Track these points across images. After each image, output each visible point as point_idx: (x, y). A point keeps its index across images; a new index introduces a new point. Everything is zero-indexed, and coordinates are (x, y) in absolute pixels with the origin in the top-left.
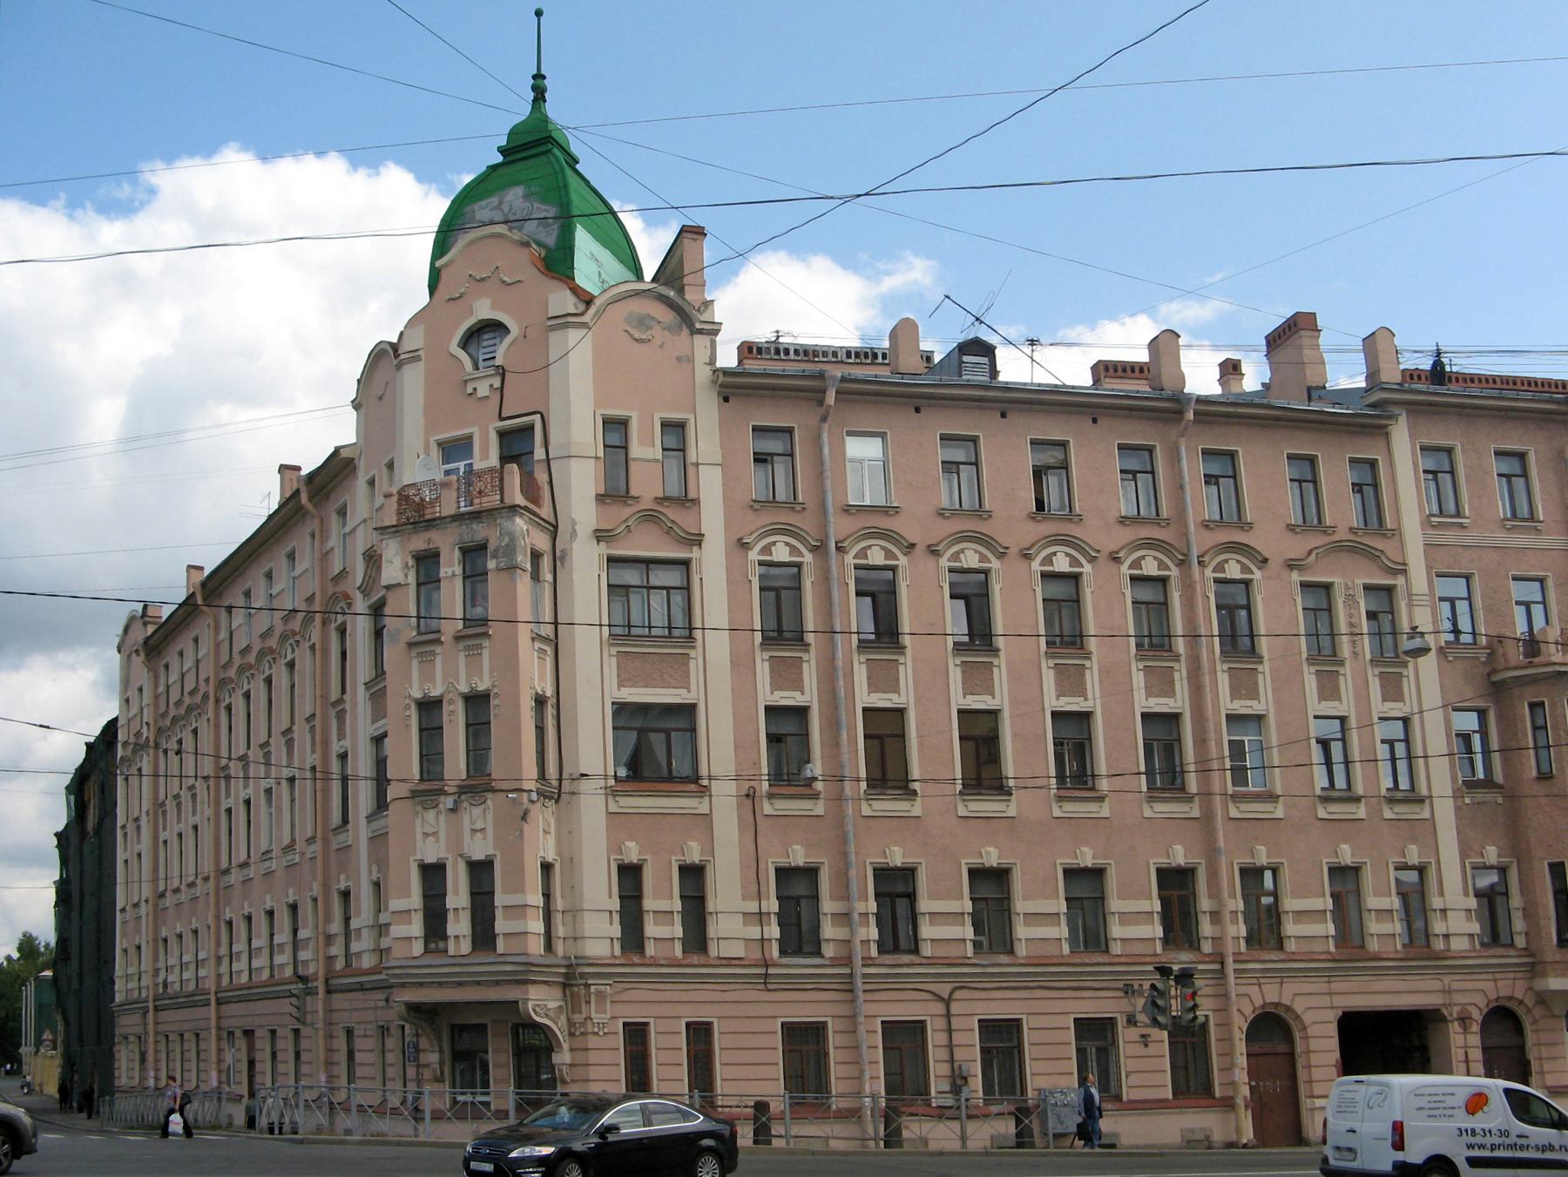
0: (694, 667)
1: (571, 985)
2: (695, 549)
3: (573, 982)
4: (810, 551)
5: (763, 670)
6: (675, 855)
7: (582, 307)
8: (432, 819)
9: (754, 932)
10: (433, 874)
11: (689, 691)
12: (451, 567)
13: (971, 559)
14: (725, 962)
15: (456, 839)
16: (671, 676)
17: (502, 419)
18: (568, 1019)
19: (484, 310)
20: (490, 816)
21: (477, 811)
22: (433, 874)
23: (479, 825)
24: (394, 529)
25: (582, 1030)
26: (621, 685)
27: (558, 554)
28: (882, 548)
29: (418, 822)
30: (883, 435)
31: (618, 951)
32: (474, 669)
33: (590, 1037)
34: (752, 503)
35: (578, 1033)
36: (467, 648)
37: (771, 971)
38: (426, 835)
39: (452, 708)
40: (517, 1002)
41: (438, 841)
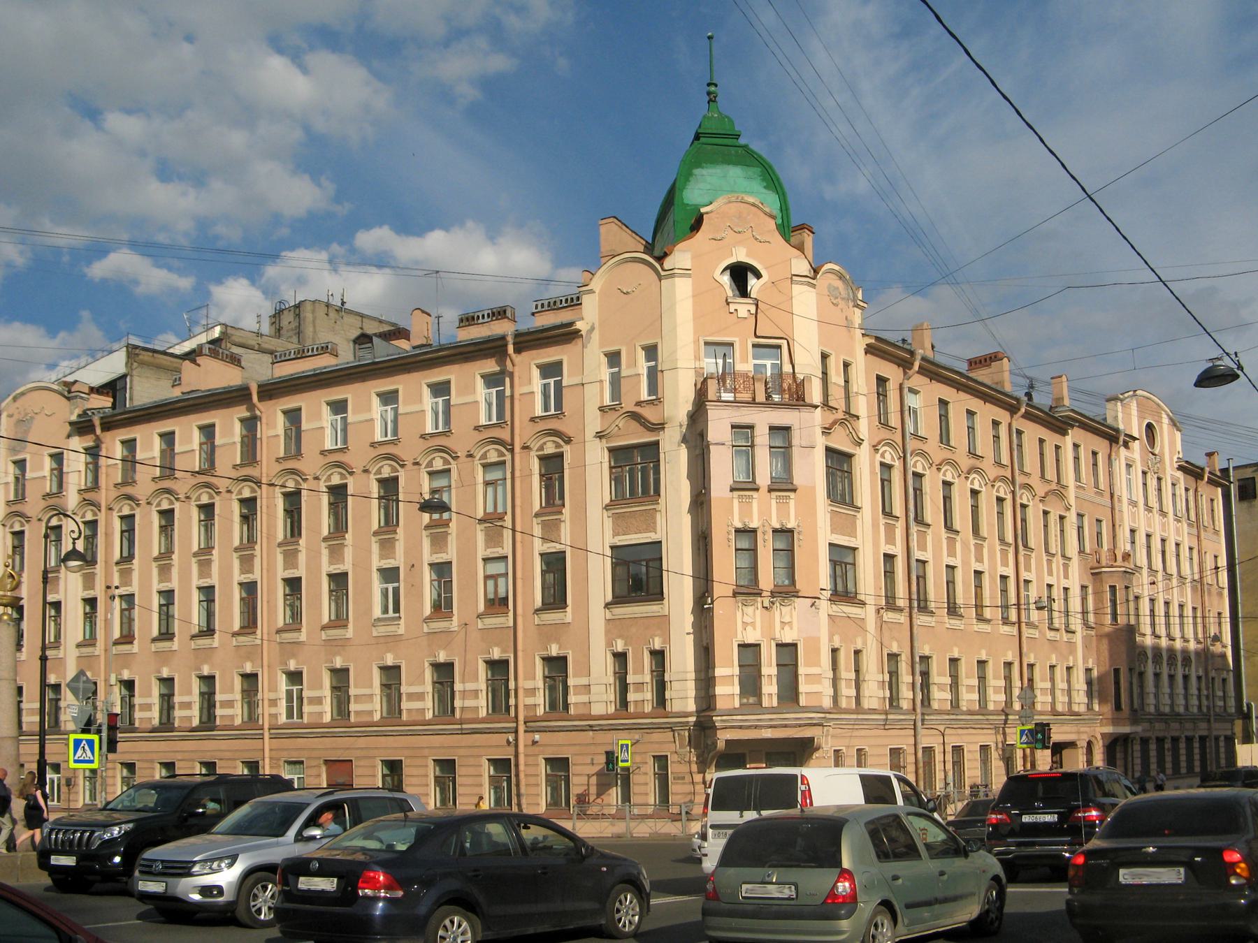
12: (762, 437)
19: (741, 255)
22: (750, 651)
23: (787, 619)
29: (739, 614)
41: (755, 629)
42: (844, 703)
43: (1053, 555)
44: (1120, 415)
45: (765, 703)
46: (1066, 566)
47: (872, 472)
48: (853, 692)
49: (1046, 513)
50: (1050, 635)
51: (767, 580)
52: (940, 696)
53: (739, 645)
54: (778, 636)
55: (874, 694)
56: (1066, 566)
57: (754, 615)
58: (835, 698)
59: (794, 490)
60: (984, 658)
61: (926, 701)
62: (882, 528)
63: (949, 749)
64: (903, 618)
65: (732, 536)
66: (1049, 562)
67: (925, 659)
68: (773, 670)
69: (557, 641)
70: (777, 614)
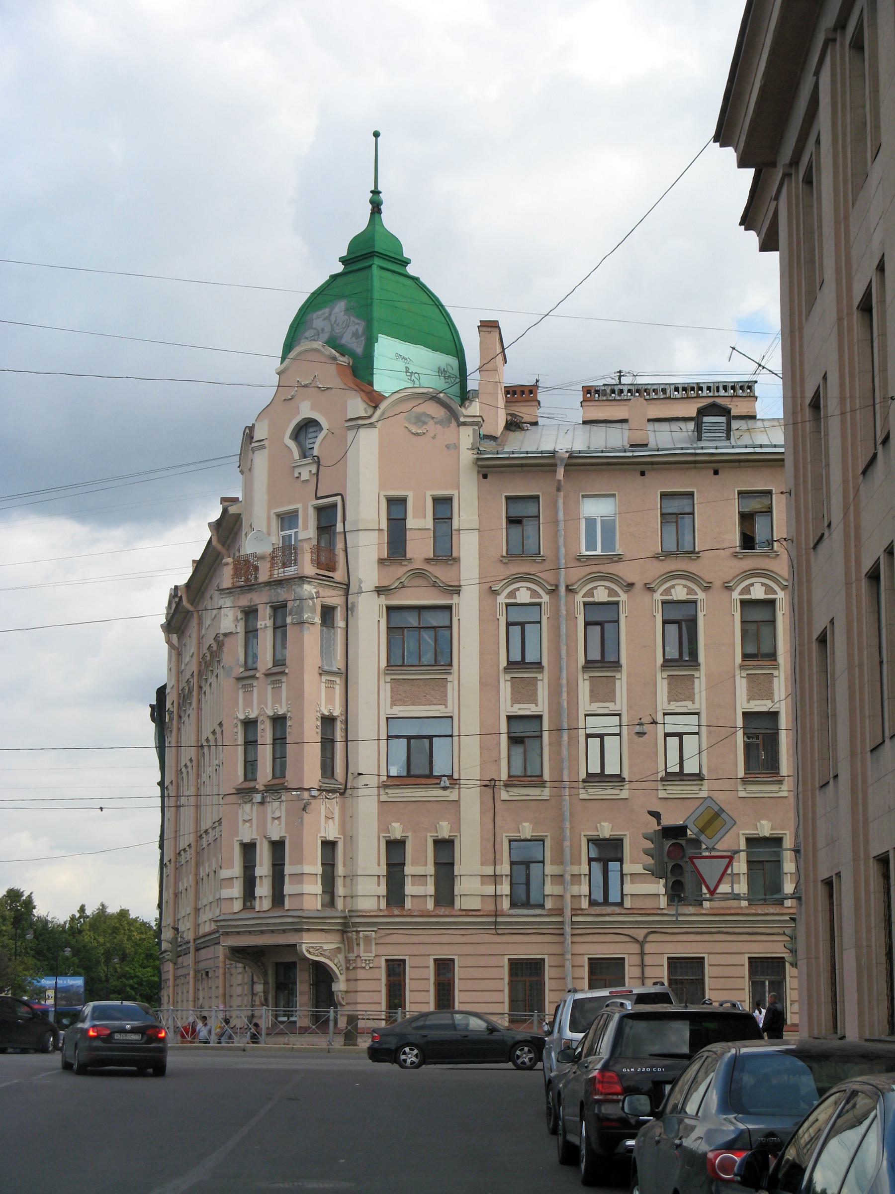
0: (451, 689)
1: (347, 932)
2: (455, 596)
3: (348, 930)
4: (547, 593)
5: (505, 689)
6: (430, 832)
7: (370, 411)
8: (248, 810)
9: (489, 890)
10: (249, 849)
11: (446, 707)
12: (264, 621)
13: (680, 593)
14: (464, 913)
16: (432, 696)
17: (317, 498)
18: (346, 957)
19: (306, 411)
21: (276, 804)
22: (249, 849)
23: (277, 814)
24: (228, 591)
25: (354, 965)
26: (393, 704)
27: (349, 606)
28: (606, 587)
29: (240, 812)
30: (614, 495)
31: (383, 905)
33: (359, 971)
34: (501, 559)
35: (351, 968)
36: (273, 682)
37: (499, 919)
38: (245, 821)
39: (262, 727)
40: (296, 945)
41: (251, 826)
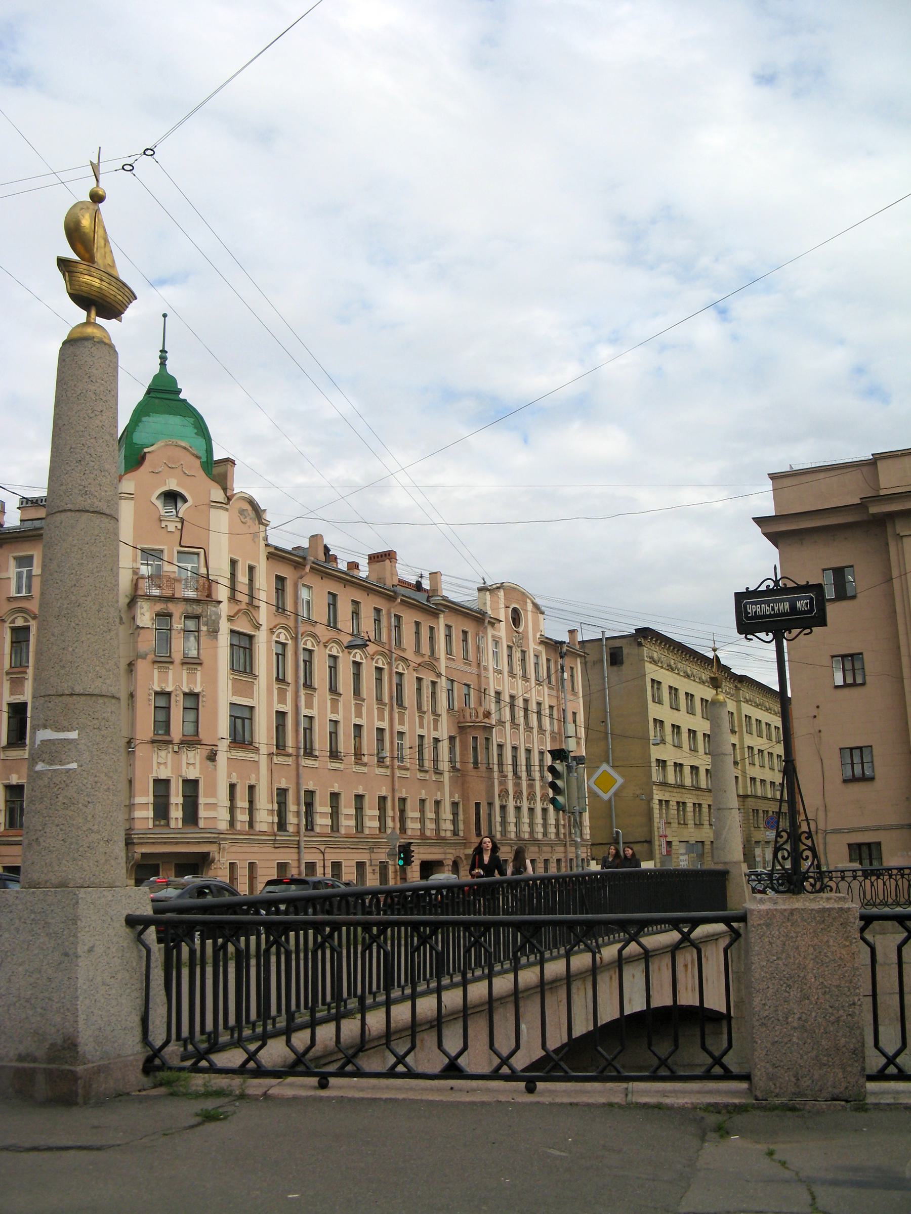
8: (165, 756)
15: (177, 767)
20: (198, 757)
21: (191, 754)
22: (162, 785)
23: (192, 761)
29: (155, 756)
32: (192, 679)
42: (238, 826)
43: (424, 713)
44: (488, 603)
45: (173, 824)
46: (436, 722)
47: (269, 649)
48: (246, 818)
49: (419, 680)
50: (420, 775)
51: (177, 731)
52: (322, 821)
53: (154, 780)
54: (184, 774)
55: (265, 819)
56: (436, 722)
57: (167, 756)
58: (232, 822)
59: (201, 664)
60: (361, 793)
61: (310, 826)
62: (275, 692)
63: (328, 864)
64: (290, 761)
65: (152, 697)
66: (421, 718)
67: (310, 794)
68: (180, 800)
69: (17, 772)
70: (184, 757)
